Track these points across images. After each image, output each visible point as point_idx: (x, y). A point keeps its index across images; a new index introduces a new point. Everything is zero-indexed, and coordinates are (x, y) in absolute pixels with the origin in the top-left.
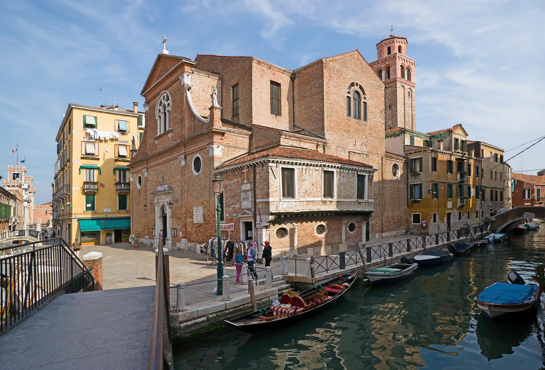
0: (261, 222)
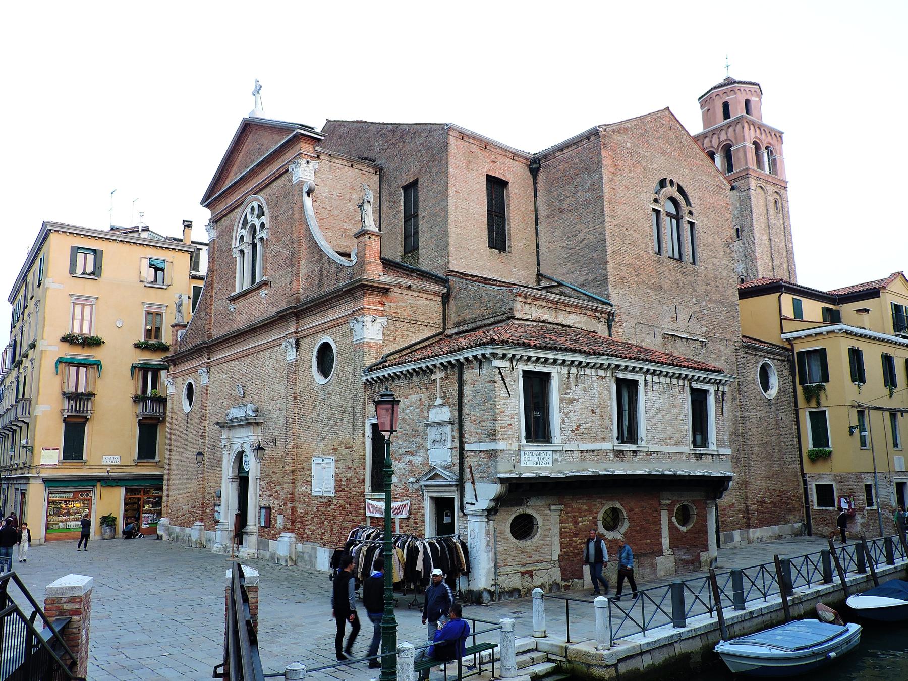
0: (476, 500)
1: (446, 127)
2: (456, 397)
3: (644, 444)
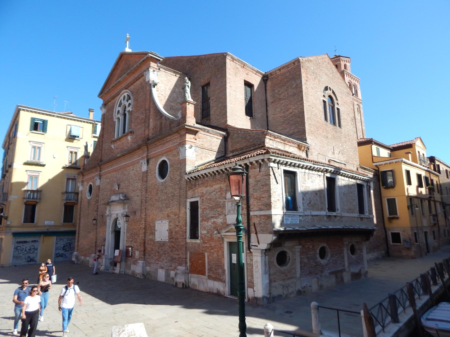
1: (225, 54)
3: (339, 212)
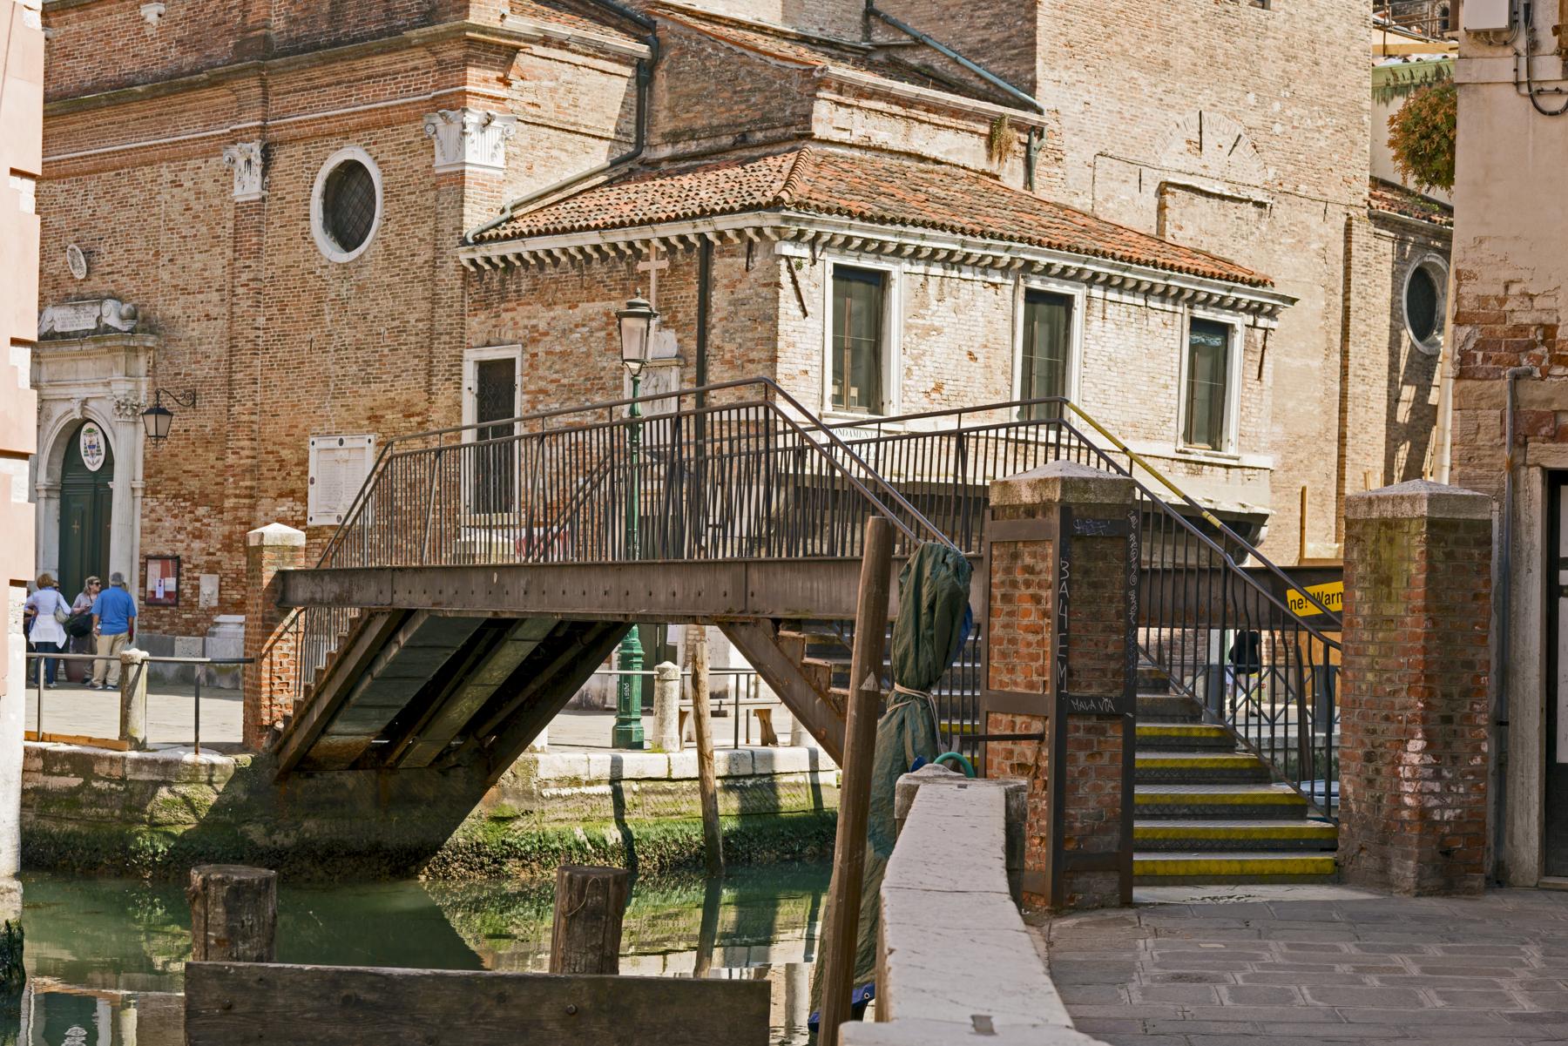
2: (694, 311)
